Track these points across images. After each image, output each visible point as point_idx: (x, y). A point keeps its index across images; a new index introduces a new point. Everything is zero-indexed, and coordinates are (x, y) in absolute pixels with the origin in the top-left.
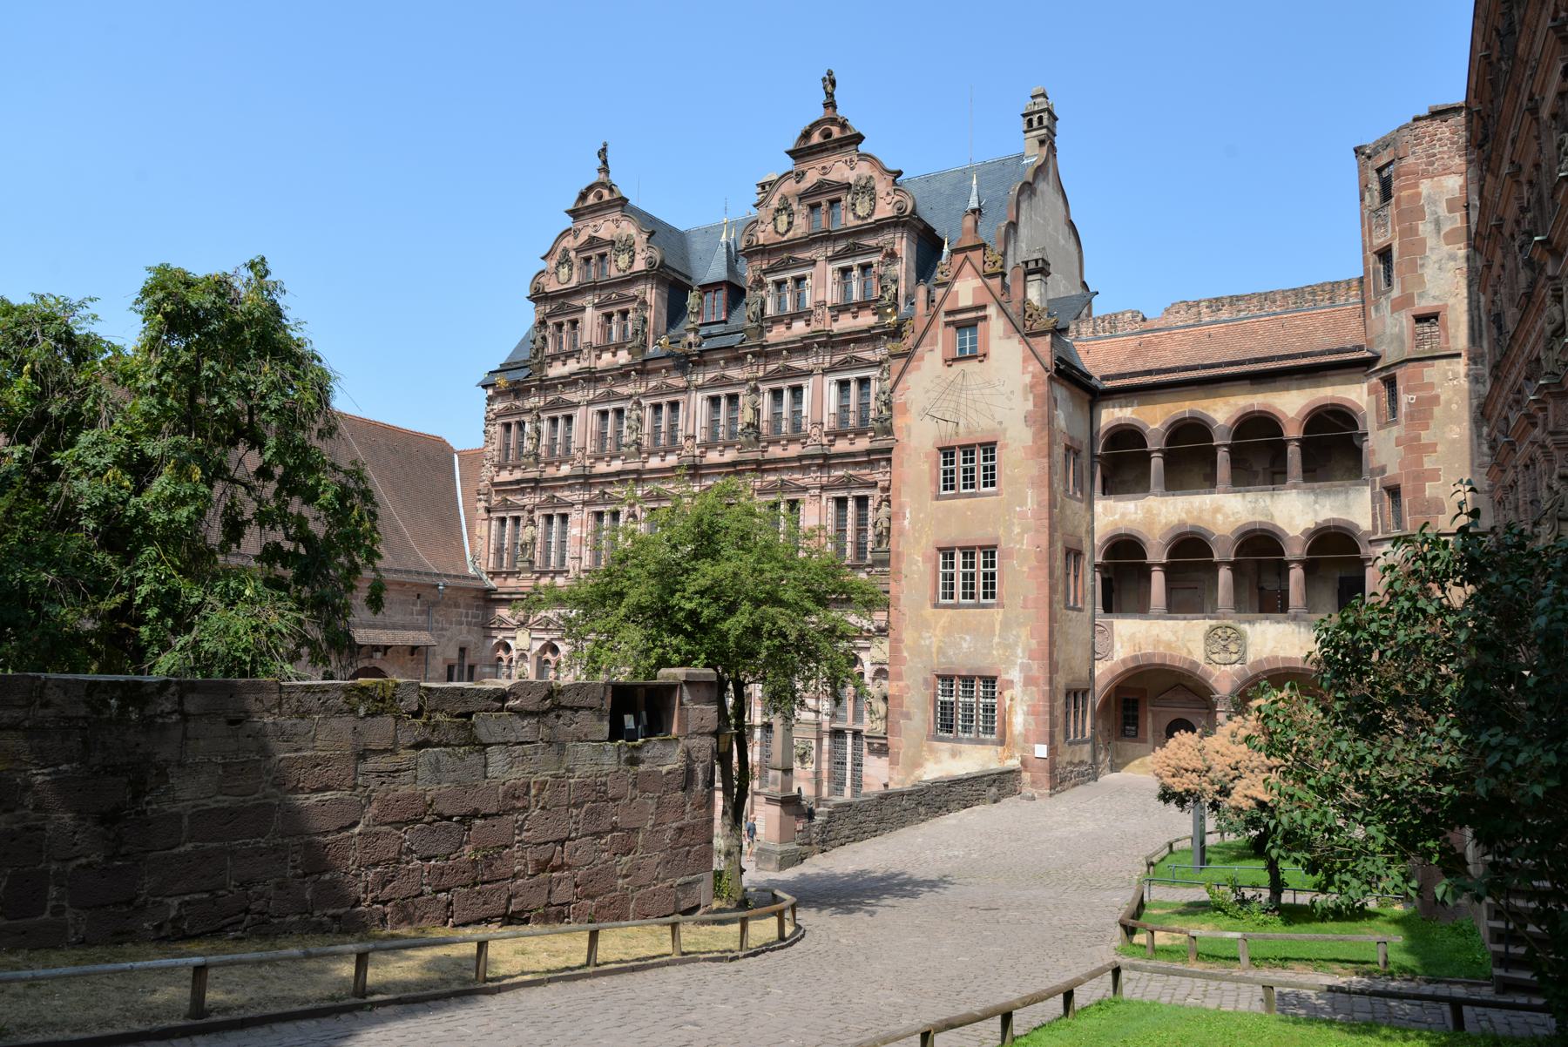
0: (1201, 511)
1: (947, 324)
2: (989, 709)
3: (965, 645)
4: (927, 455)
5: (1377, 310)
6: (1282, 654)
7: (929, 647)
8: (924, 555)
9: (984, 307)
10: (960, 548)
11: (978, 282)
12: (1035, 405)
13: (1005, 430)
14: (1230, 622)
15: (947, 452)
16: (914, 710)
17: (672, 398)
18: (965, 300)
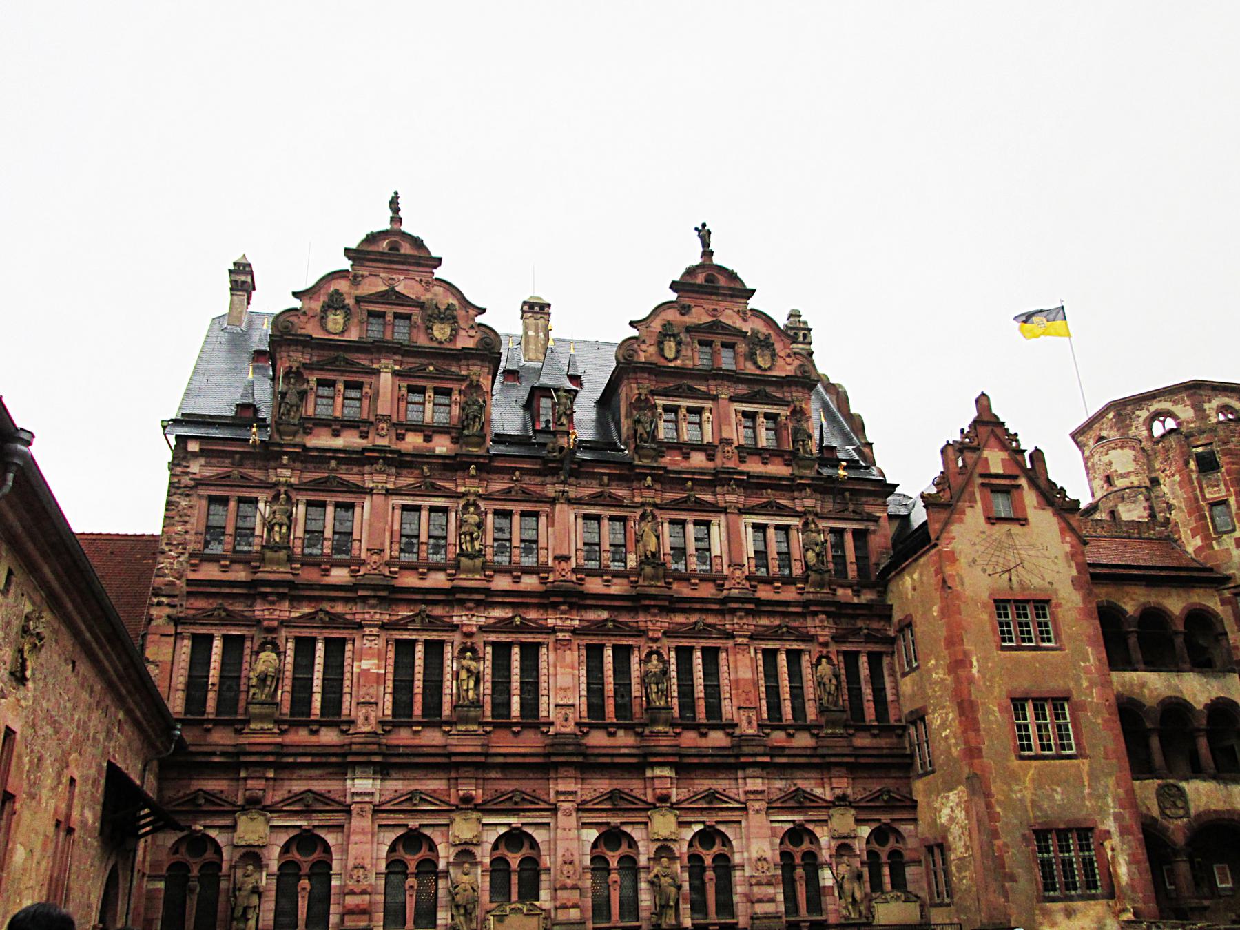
0: (1132, 685)
1: (983, 485)
2: (1088, 864)
3: (1058, 797)
4: (984, 605)
5: (1219, 544)
6: (1213, 807)
7: (1022, 800)
8: (999, 705)
9: (1016, 477)
10: (1033, 699)
11: (1003, 455)
12: (1079, 572)
13: (1056, 591)
14: (1172, 781)
15: (1000, 604)
16: (1019, 871)
17: (528, 507)
18: (996, 468)
